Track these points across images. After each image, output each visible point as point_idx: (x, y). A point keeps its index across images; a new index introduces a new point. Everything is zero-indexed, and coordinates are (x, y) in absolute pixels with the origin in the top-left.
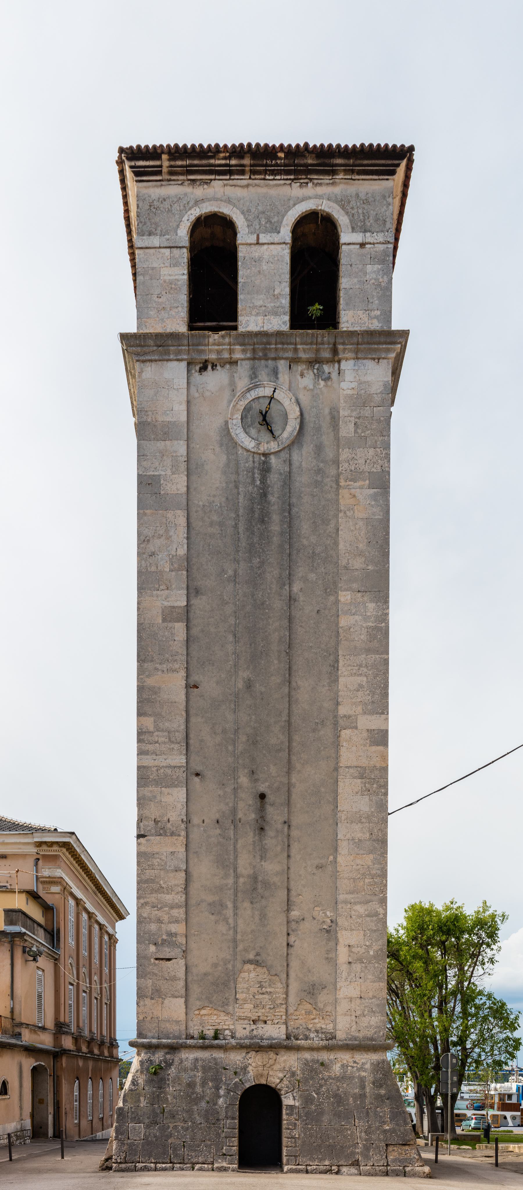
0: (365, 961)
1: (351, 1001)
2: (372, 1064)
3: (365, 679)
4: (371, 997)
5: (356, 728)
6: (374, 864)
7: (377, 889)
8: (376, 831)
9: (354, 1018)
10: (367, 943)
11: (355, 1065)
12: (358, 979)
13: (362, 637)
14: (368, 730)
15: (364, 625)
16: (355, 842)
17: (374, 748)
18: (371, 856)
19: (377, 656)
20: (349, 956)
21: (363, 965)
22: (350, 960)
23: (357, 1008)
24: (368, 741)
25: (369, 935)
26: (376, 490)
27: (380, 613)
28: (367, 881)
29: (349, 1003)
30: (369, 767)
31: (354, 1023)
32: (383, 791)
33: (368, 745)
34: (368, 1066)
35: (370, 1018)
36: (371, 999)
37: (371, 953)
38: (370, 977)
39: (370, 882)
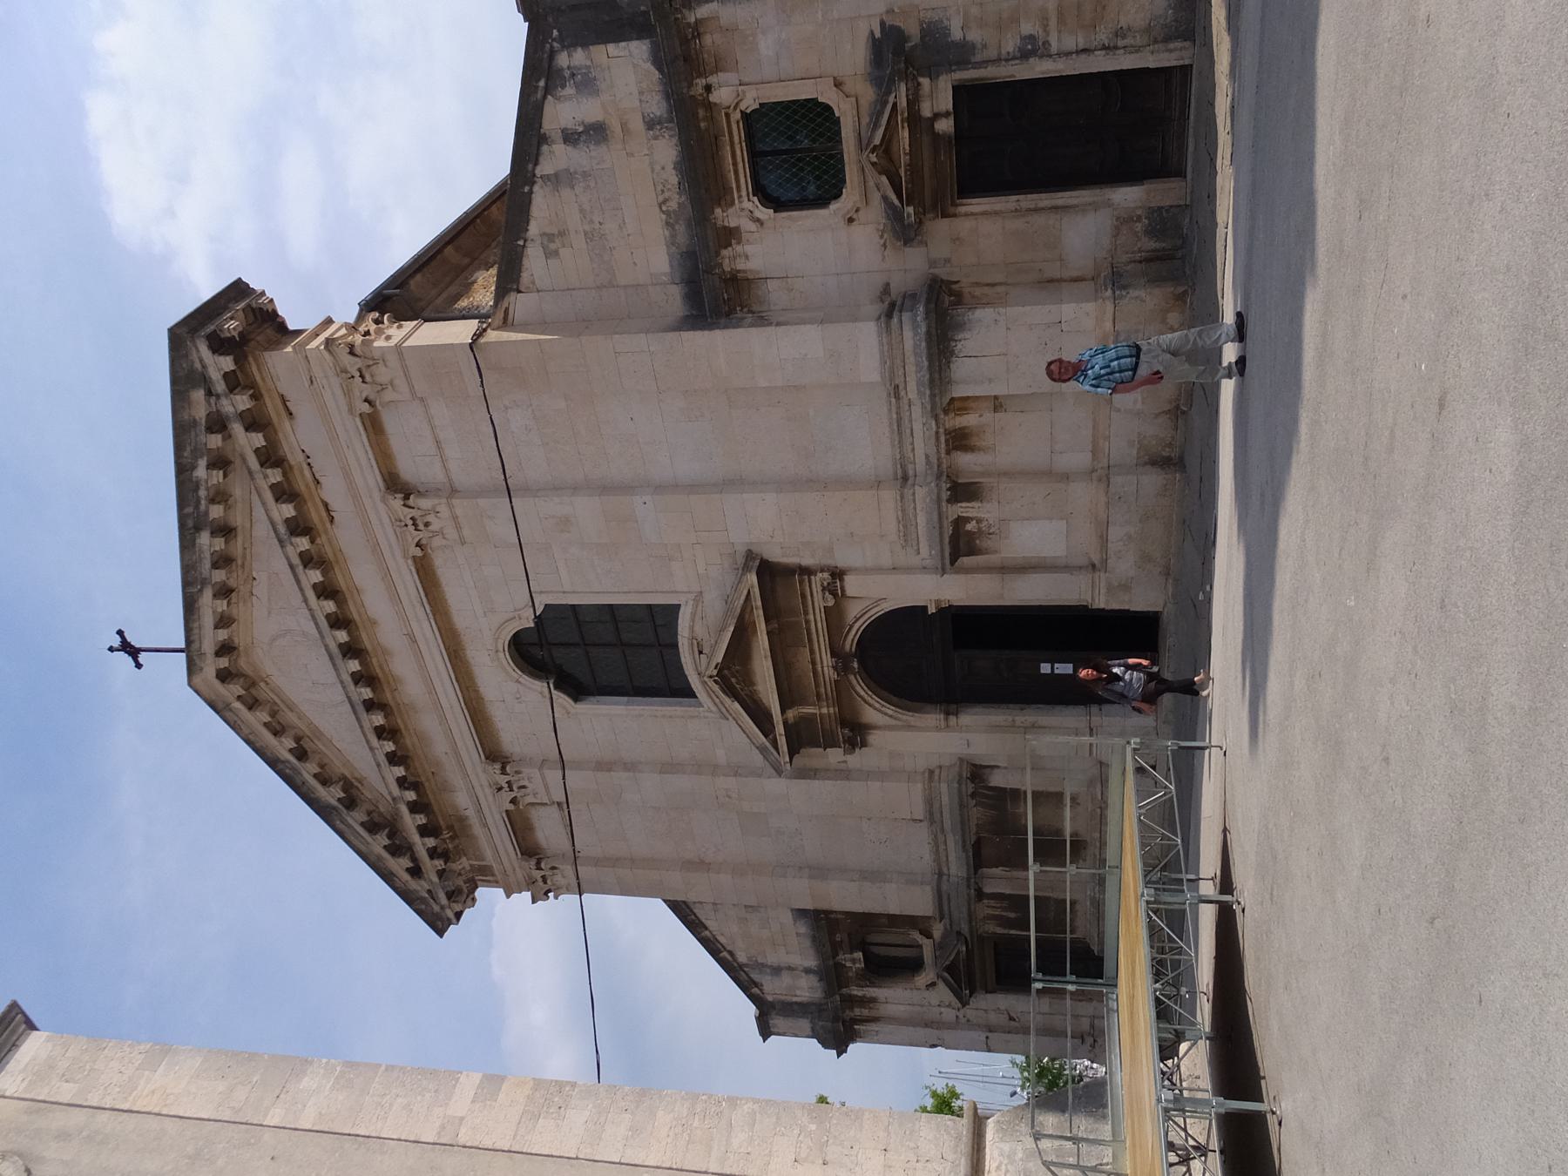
0: (826, 1138)
1: (890, 1167)
2: (1002, 1140)
3: (399, 1100)
4: (886, 1135)
5: (462, 1119)
6: (673, 1111)
7: (713, 1110)
8: (624, 1104)
9: (919, 1165)
10: (796, 1132)
11: (1003, 1167)
12: (853, 1152)
13: (341, 1098)
14: (473, 1102)
15: (327, 1093)
16: (632, 1136)
17: (501, 1096)
18: (660, 1113)
19: (377, 1079)
20: (813, 1162)
21: (831, 1141)
22: (821, 1162)
23: (902, 1157)
24: (488, 1103)
25: (783, 1129)
26: (164, 1063)
27: (322, 1071)
28: (696, 1124)
29: (892, 1169)
30: (526, 1106)
31: (928, 1164)
32: (567, 1089)
33: (494, 1103)
34: (1006, 1147)
35: (922, 1139)
36: (889, 1133)
37: (813, 1127)
38: (852, 1133)
39: (700, 1119)
